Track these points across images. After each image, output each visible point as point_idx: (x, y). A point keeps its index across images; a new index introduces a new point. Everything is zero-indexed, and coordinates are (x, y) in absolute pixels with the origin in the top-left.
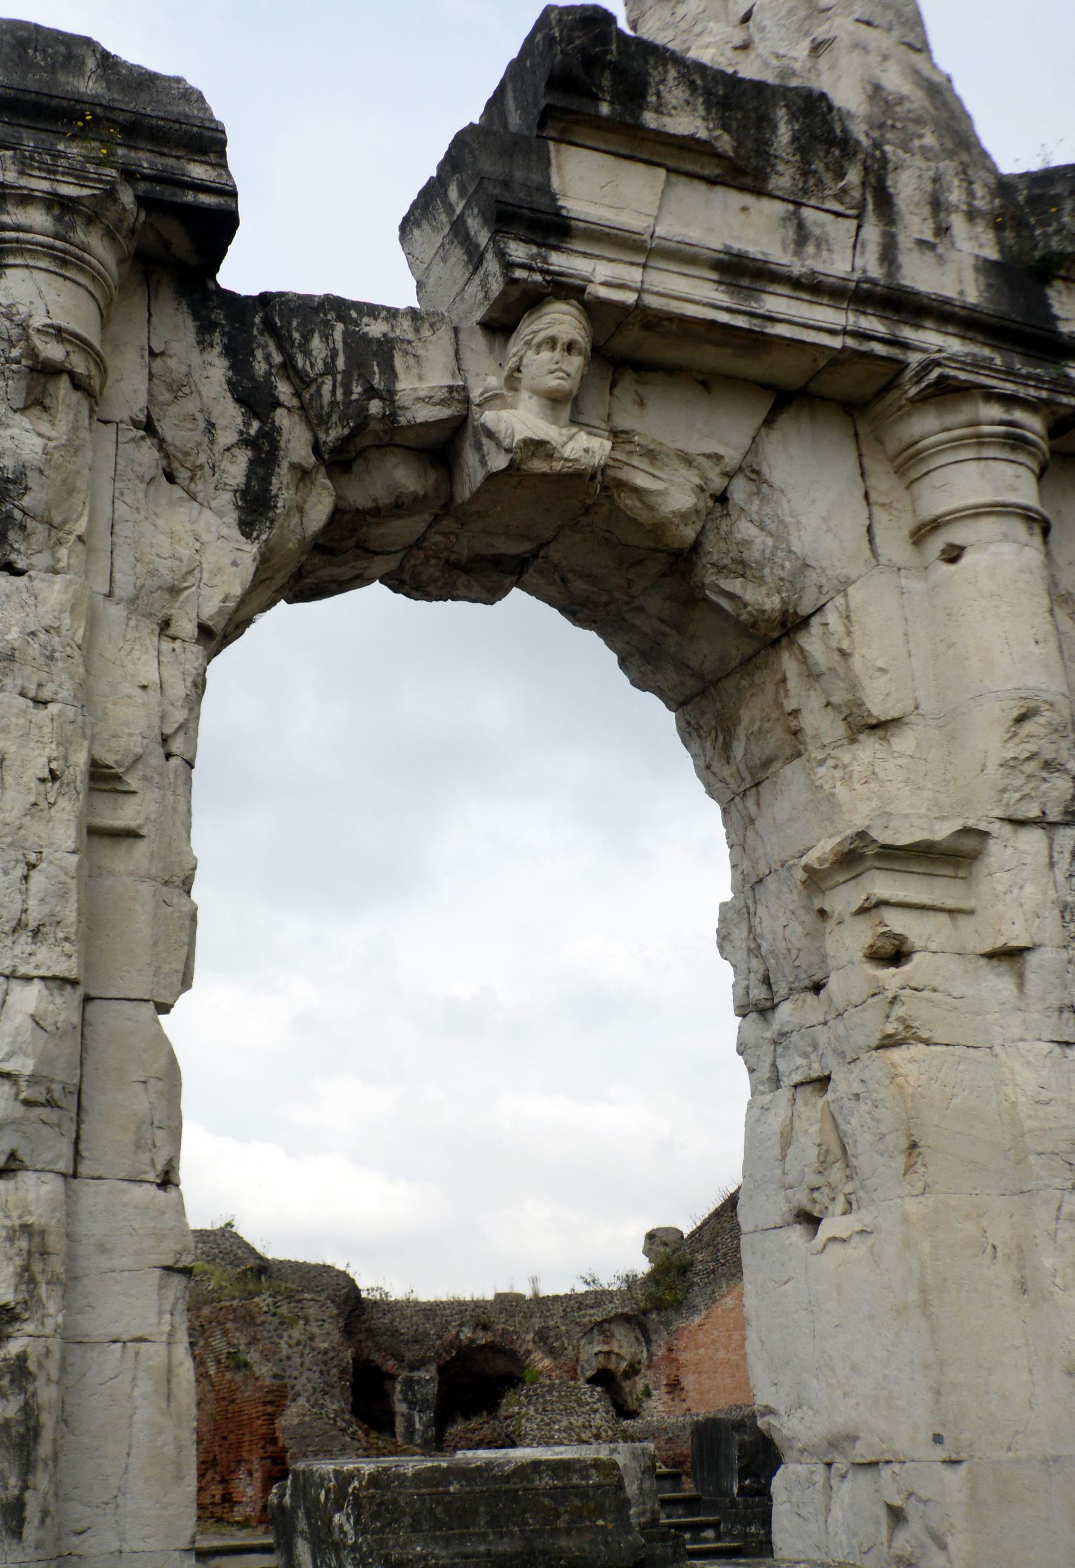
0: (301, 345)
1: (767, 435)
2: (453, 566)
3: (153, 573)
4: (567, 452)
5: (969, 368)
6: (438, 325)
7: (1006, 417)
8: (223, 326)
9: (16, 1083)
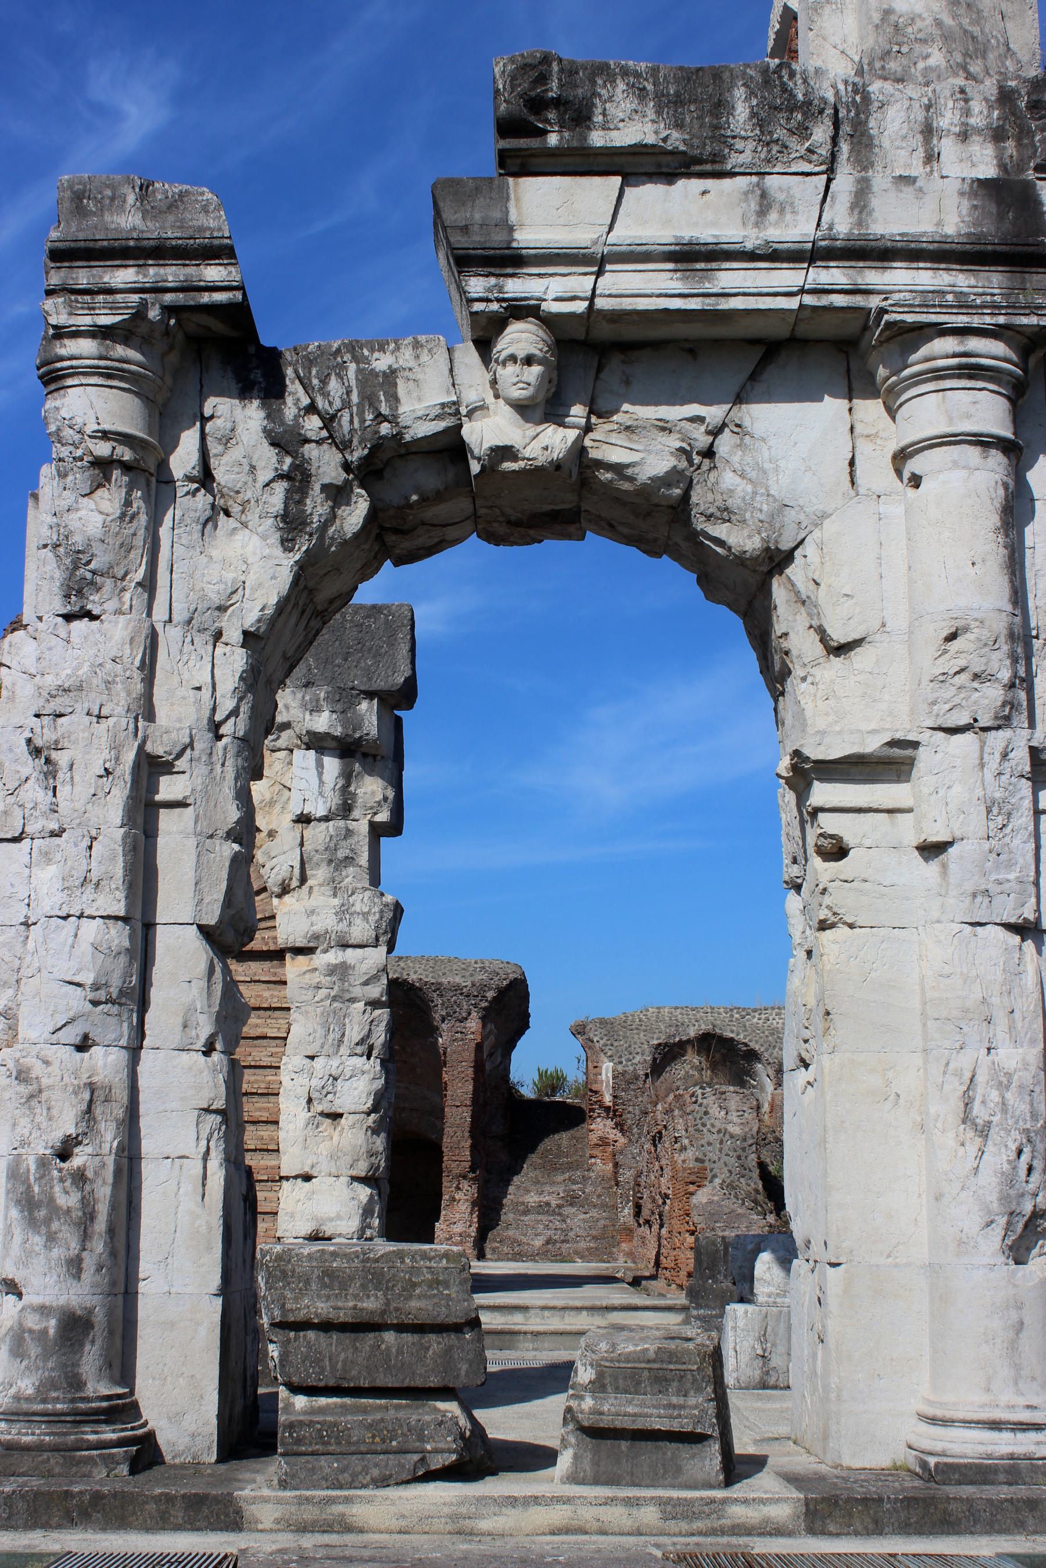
0: (321, 389)
1: (752, 389)
2: (517, 524)
3: (203, 598)
5: (918, 310)
6: (435, 350)
8: (260, 383)
9: (84, 989)
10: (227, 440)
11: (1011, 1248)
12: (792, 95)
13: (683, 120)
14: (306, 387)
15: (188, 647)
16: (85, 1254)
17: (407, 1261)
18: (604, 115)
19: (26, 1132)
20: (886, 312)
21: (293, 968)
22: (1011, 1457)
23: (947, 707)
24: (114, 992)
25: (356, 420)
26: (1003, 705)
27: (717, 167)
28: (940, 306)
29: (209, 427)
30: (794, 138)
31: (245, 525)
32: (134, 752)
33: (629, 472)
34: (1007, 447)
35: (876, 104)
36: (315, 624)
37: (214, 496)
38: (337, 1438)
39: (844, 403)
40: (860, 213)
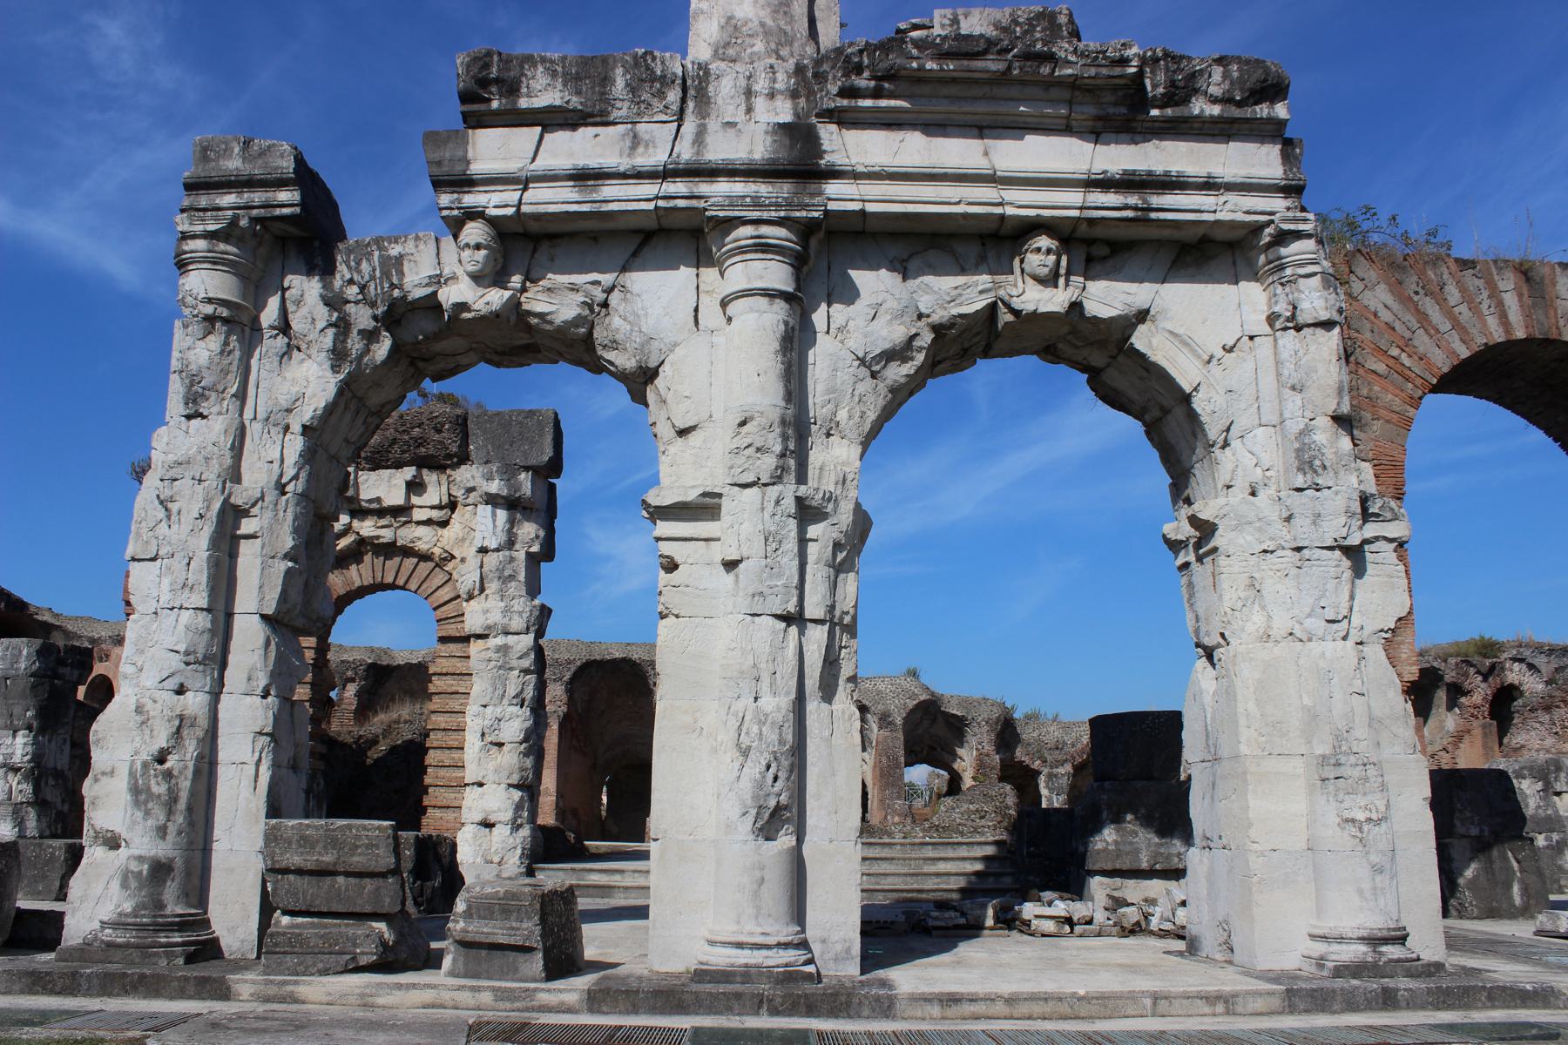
2: (503, 353)
4: (475, 307)
7: (756, 233)
10: (298, 303)
11: (760, 830)
12: (653, 72)
13: (581, 90)
14: (349, 267)
15: (266, 436)
16: (169, 824)
17: (354, 831)
18: (528, 88)
19: (138, 745)
20: (707, 210)
21: (475, 647)
22: (746, 966)
23: (740, 470)
24: (200, 657)
25: (379, 288)
26: (776, 468)
27: (604, 119)
28: (742, 205)
29: (287, 294)
30: (656, 100)
32: (220, 503)
33: (549, 318)
35: (714, 76)
36: (373, 420)
37: (290, 339)
38: (301, 944)
39: (694, 271)
40: (699, 146)
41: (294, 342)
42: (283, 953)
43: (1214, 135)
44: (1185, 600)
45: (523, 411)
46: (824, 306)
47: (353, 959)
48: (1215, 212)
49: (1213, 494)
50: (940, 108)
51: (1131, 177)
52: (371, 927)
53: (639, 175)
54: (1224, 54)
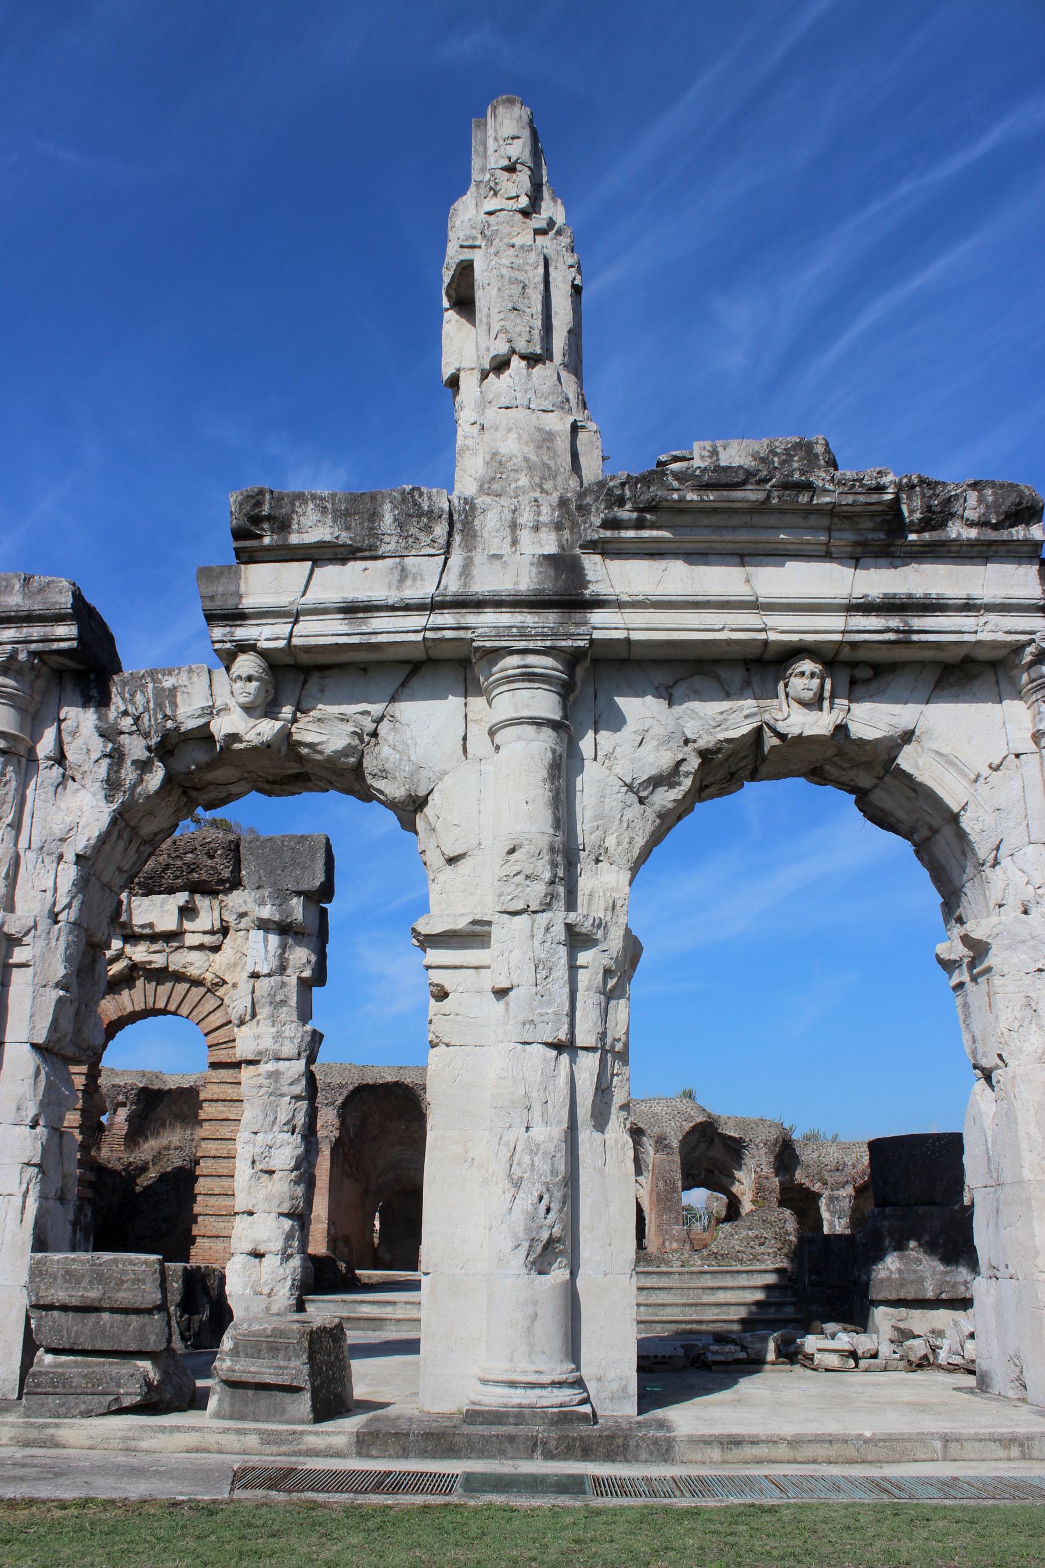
2: (273, 783)
4: (247, 738)
7: (522, 663)
10: (74, 734)
11: (533, 1263)
12: (420, 507)
14: (123, 699)
15: (40, 865)
18: (299, 524)
20: (474, 641)
21: (246, 1073)
22: (520, 1406)
23: (509, 897)
26: (546, 896)
27: (373, 553)
31: (84, 786)
33: (319, 748)
34: (554, 725)
35: (480, 511)
36: (146, 849)
37: (65, 770)
41: (69, 772)
42: (45, 1394)
43: (972, 558)
44: (961, 1020)
45: (295, 837)
46: (591, 733)
47: (117, 1400)
48: (976, 632)
49: (985, 913)
50: (702, 538)
51: (892, 601)
52: (136, 1366)
53: (407, 607)
54: (978, 479)
